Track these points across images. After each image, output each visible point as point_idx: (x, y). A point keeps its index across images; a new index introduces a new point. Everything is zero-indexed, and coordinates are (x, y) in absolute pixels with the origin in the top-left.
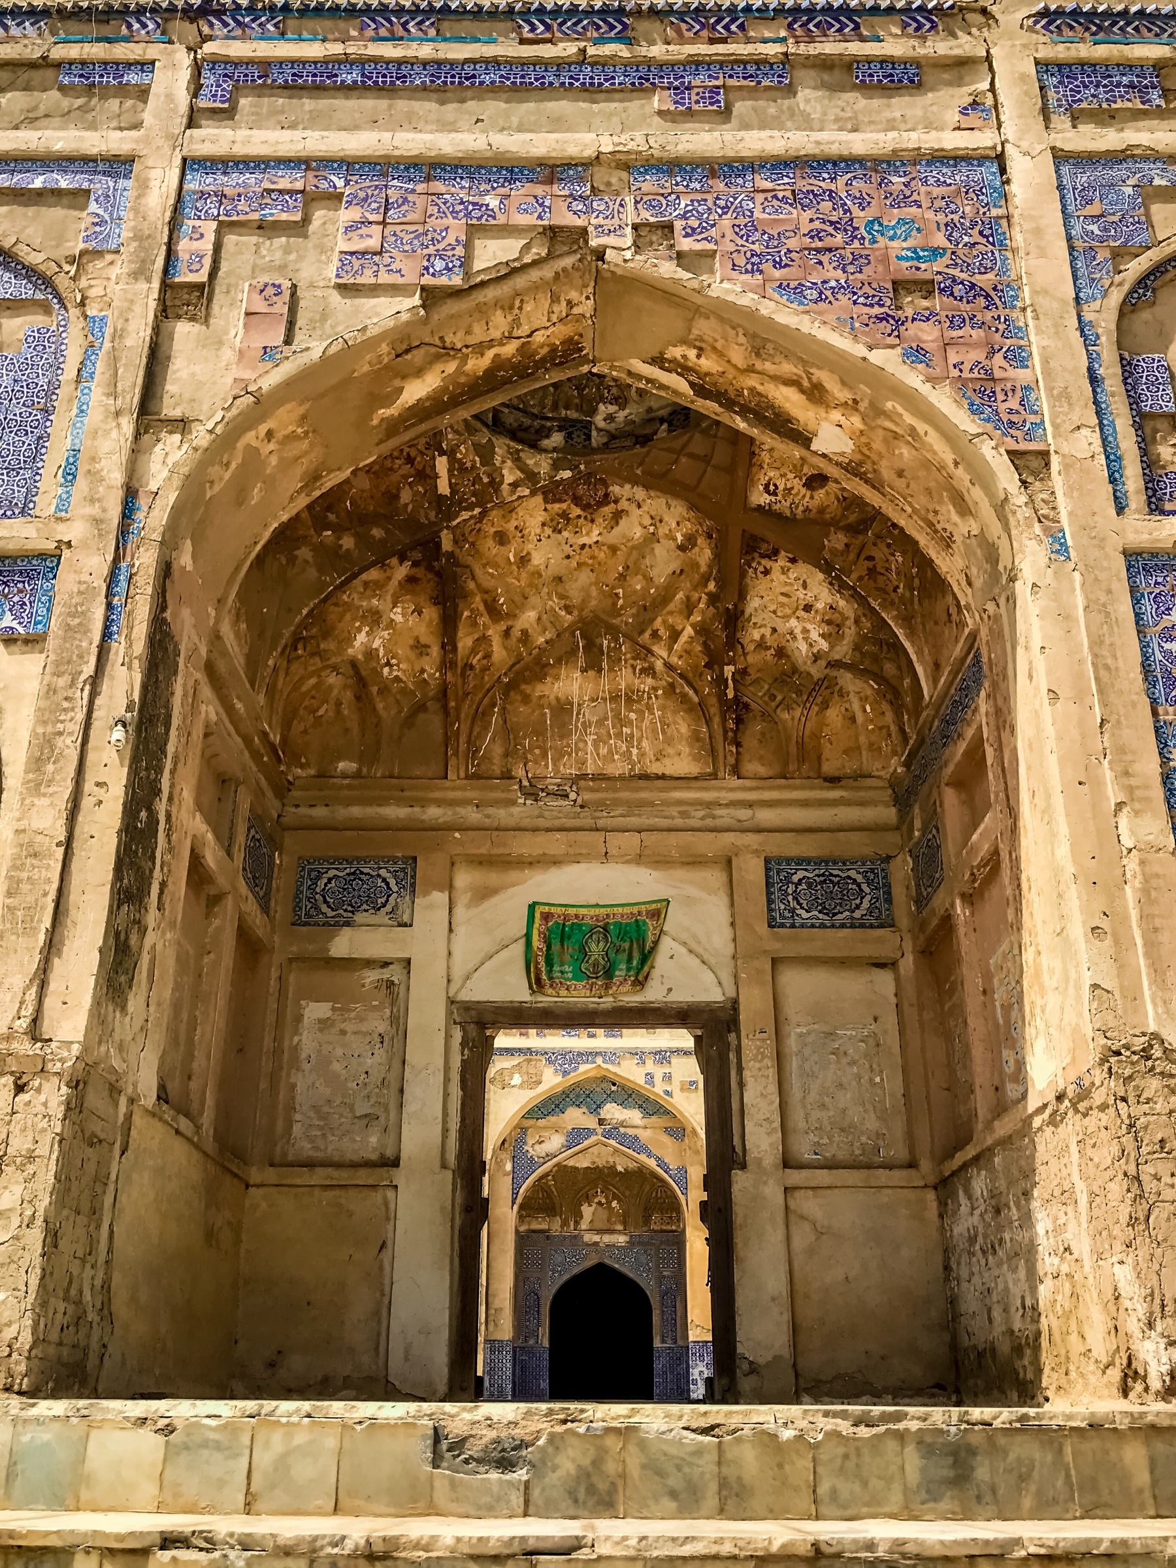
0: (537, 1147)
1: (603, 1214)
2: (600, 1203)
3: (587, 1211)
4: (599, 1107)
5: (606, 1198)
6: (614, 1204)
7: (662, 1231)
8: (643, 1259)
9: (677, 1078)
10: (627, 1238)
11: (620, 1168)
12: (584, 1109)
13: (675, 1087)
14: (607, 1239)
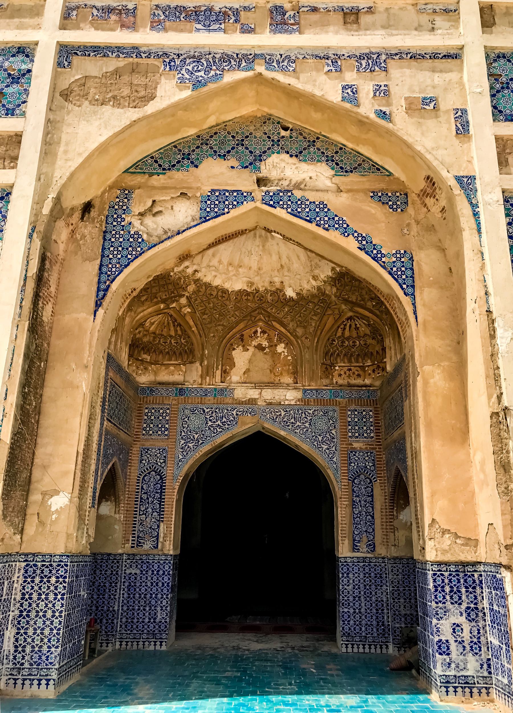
0: (149, 220)
1: (263, 362)
2: (260, 348)
3: (241, 357)
4: (260, 159)
5: (269, 339)
6: (281, 348)
7: (350, 385)
8: (322, 424)
10: (299, 395)
11: (290, 293)
12: (233, 162)
13: (398, 109)
14: (268, 394)
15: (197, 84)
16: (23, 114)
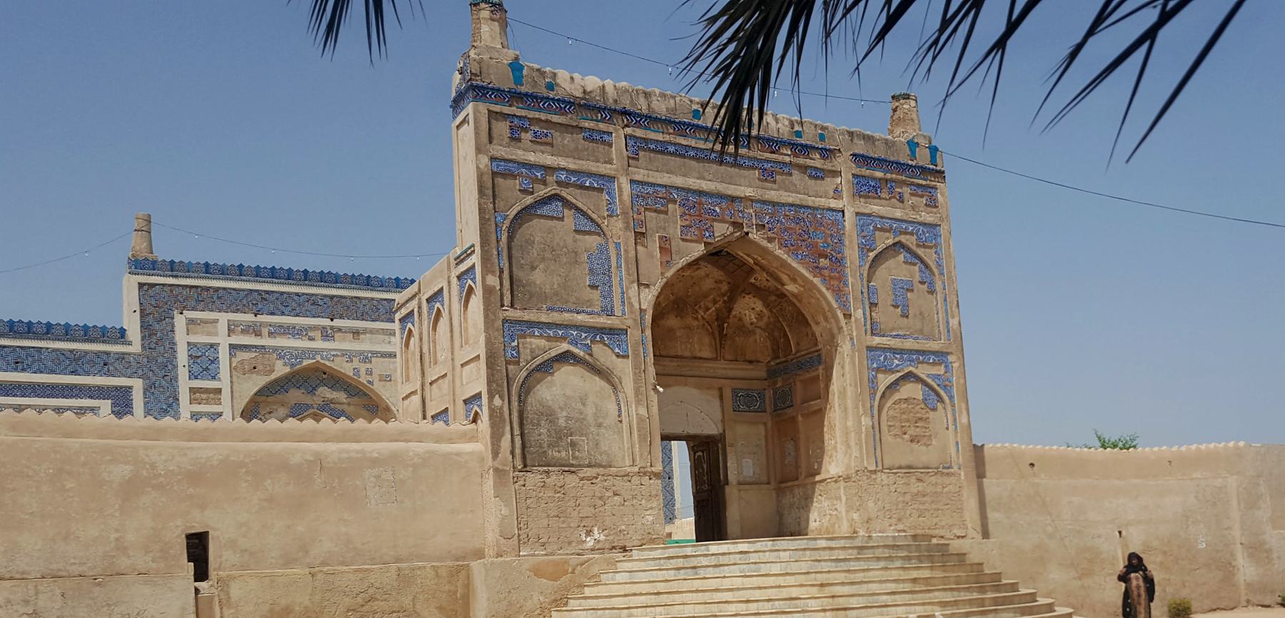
9: (376, 372)
15: (292, 365)
16: (219, 380)
